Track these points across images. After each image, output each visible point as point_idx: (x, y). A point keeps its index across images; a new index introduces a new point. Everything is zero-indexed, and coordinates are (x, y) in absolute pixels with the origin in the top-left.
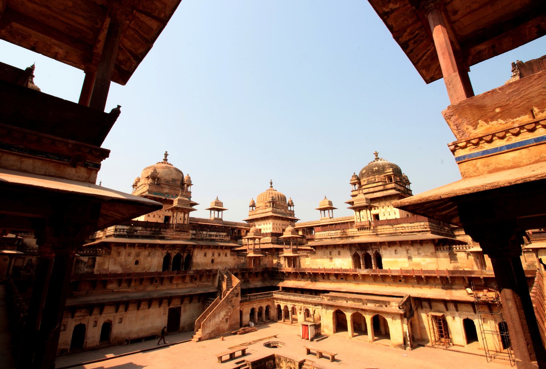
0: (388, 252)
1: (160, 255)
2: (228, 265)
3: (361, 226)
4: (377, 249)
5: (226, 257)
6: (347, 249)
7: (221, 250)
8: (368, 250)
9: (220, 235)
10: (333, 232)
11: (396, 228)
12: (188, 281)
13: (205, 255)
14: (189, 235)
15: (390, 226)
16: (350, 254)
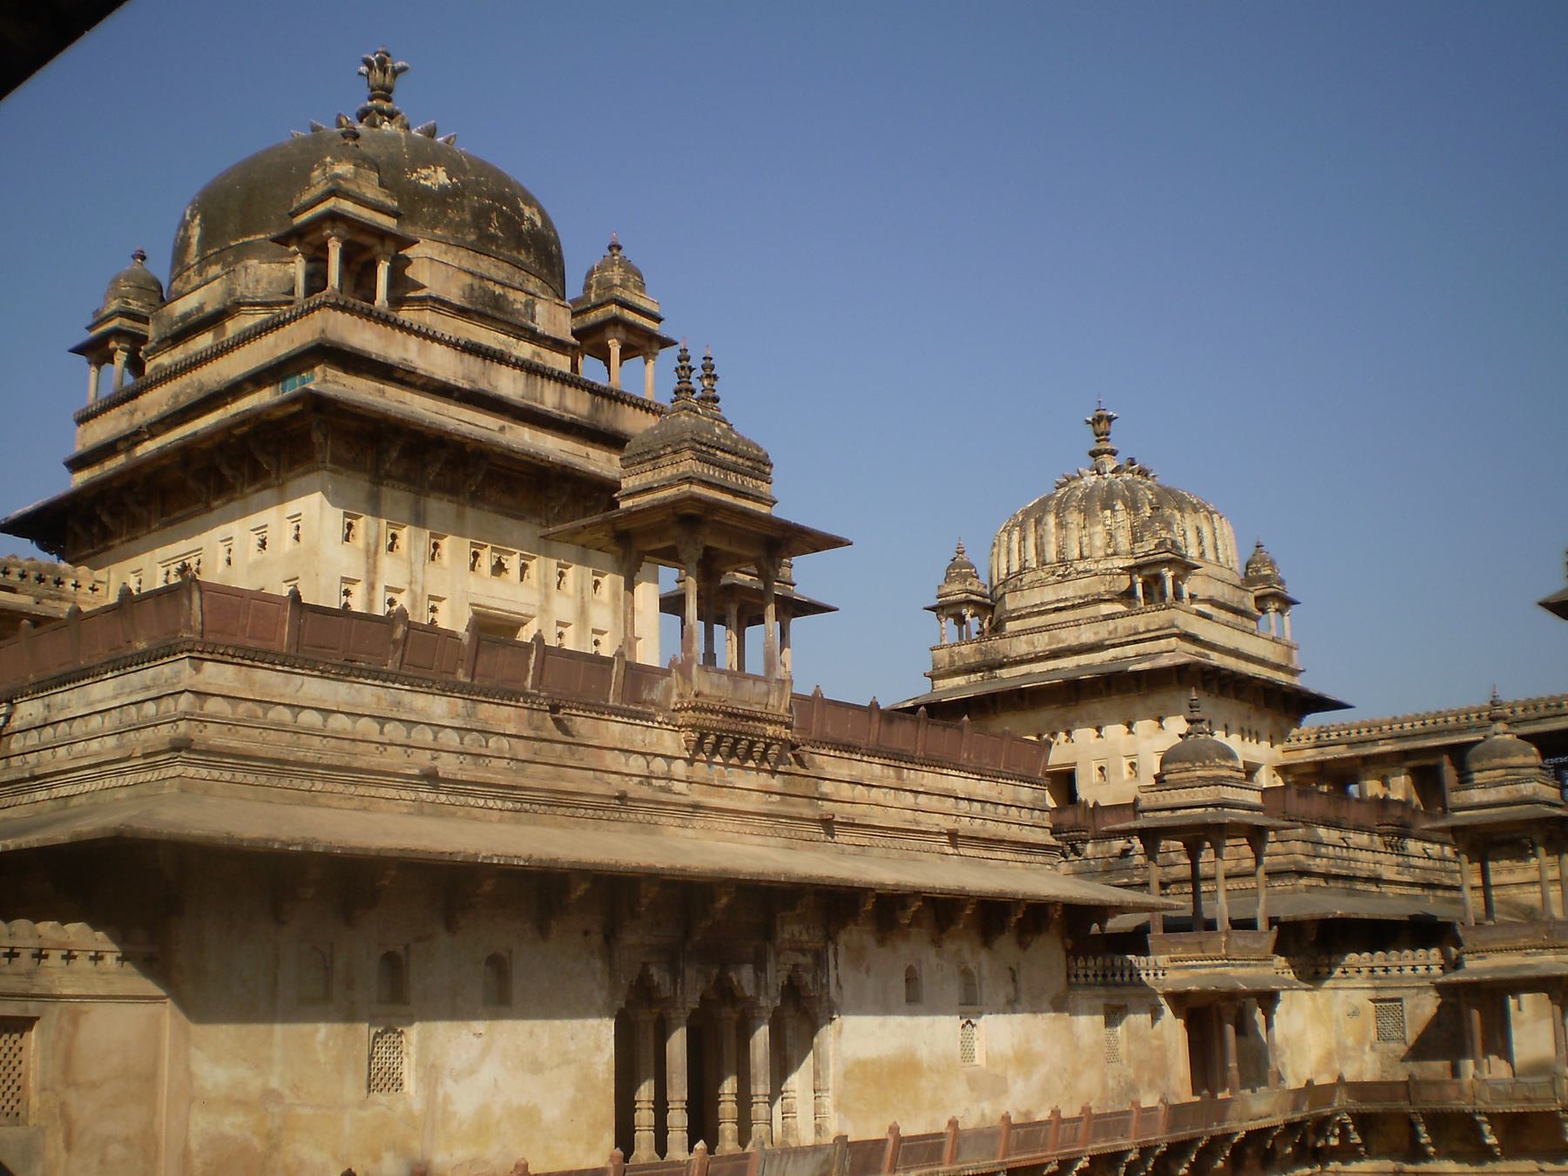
4: (803, 951)
6: (586, 933)
10: (438, 707)
15: (886, 770)
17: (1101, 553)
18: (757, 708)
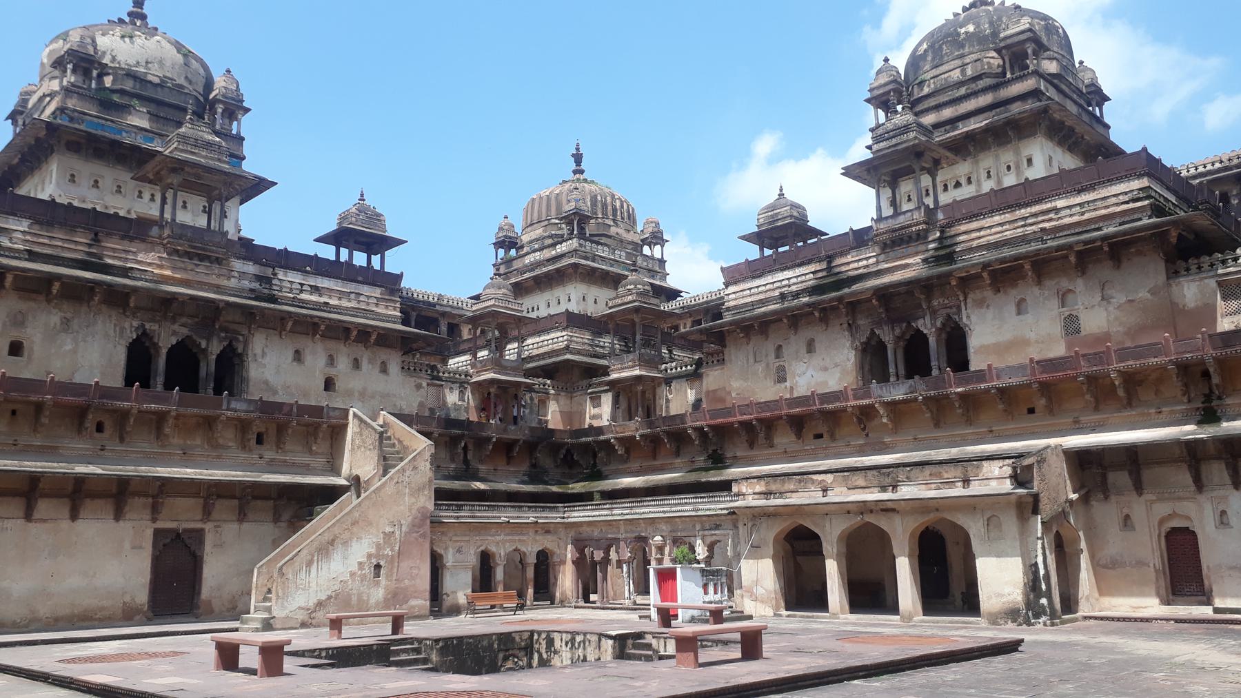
0: (989, 314)
1: (111, 332)
2: (395, 405)
4: (951, 307)
5: (382, 376)
7: (363, 349)
8: (918, 319)
9: (359, 294)
11: (1026, 218)
12: (230, 444)
13: (298, 356)
14: (229, 278)
15: (1003, 216)
16: (848, 344)
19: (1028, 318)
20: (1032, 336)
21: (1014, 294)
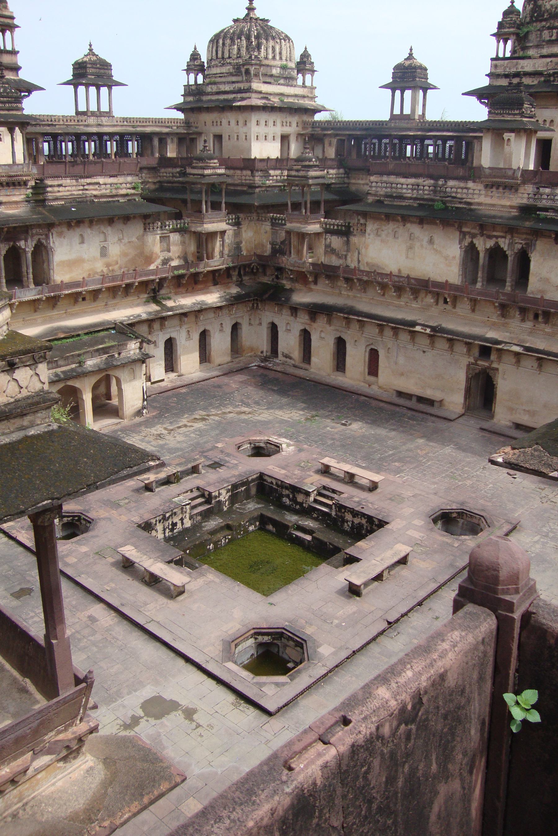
0: (65, 241)
3: (10, 177)
8: (21, 240)
11: (84, 186)
17: (235, 56)
18: (19, 173)
19: (85, 246)
20: (86, 257)
21: (78, 231)
